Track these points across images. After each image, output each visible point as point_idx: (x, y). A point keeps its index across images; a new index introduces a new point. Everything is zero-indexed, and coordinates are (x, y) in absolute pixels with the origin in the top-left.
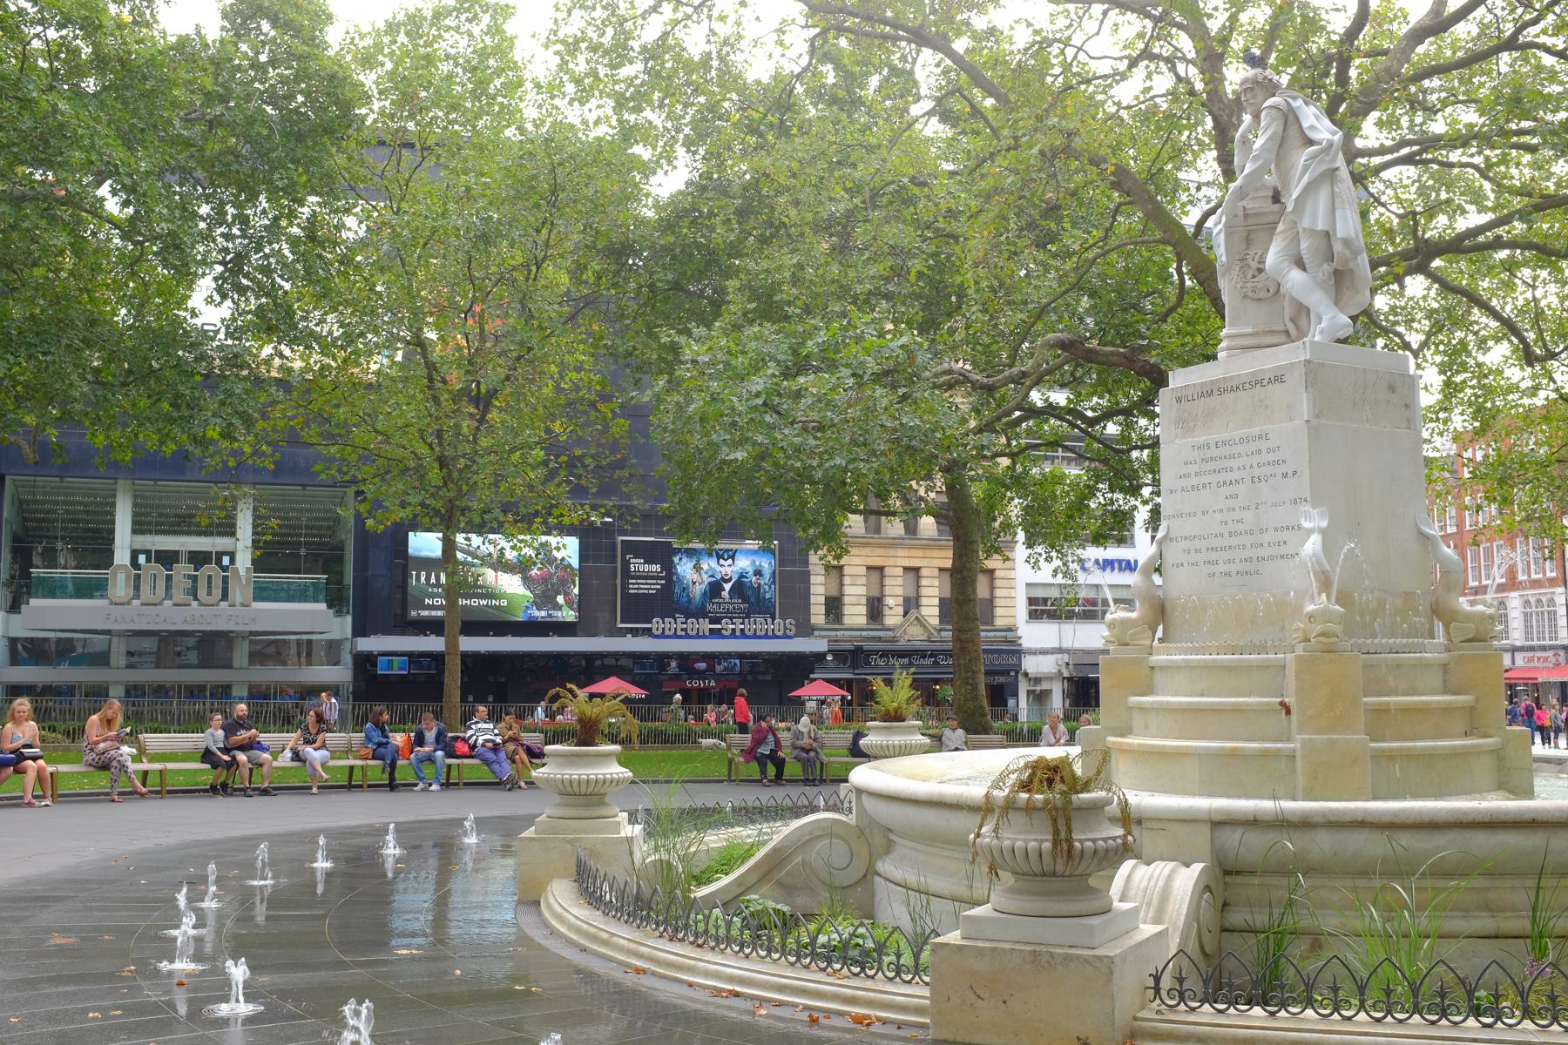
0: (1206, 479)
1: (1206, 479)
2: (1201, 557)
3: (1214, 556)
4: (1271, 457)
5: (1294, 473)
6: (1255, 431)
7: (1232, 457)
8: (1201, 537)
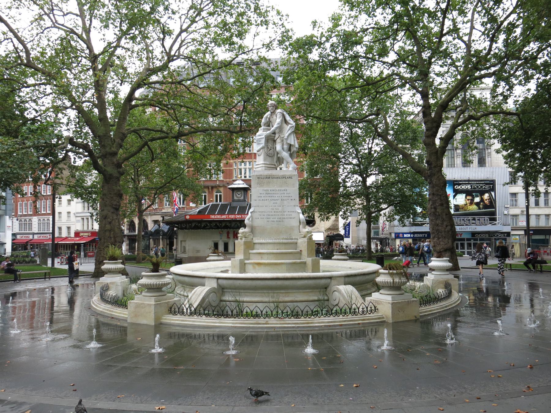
0: (266, 198)
3: (269, 217)
4: (288, 195)
6: (283, 188)
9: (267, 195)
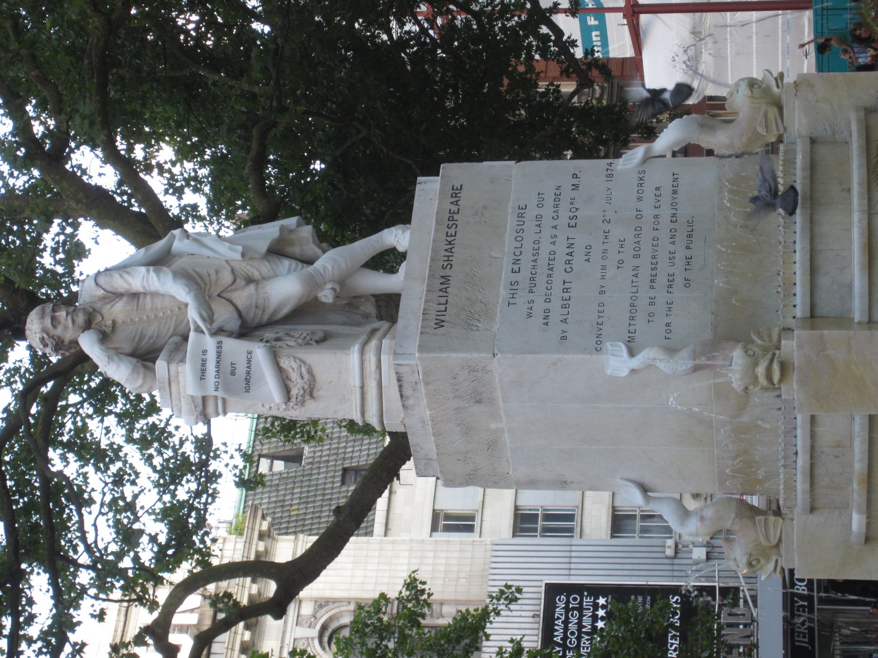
0: (558, 286)
1: (558, 286)
2: (662, 296)
3: (662, 280)
4: (549, 202)
5: (575, 176)
6: (511, 221)
7: (536, 252)
8: (634, 298)
9: (541, 288)
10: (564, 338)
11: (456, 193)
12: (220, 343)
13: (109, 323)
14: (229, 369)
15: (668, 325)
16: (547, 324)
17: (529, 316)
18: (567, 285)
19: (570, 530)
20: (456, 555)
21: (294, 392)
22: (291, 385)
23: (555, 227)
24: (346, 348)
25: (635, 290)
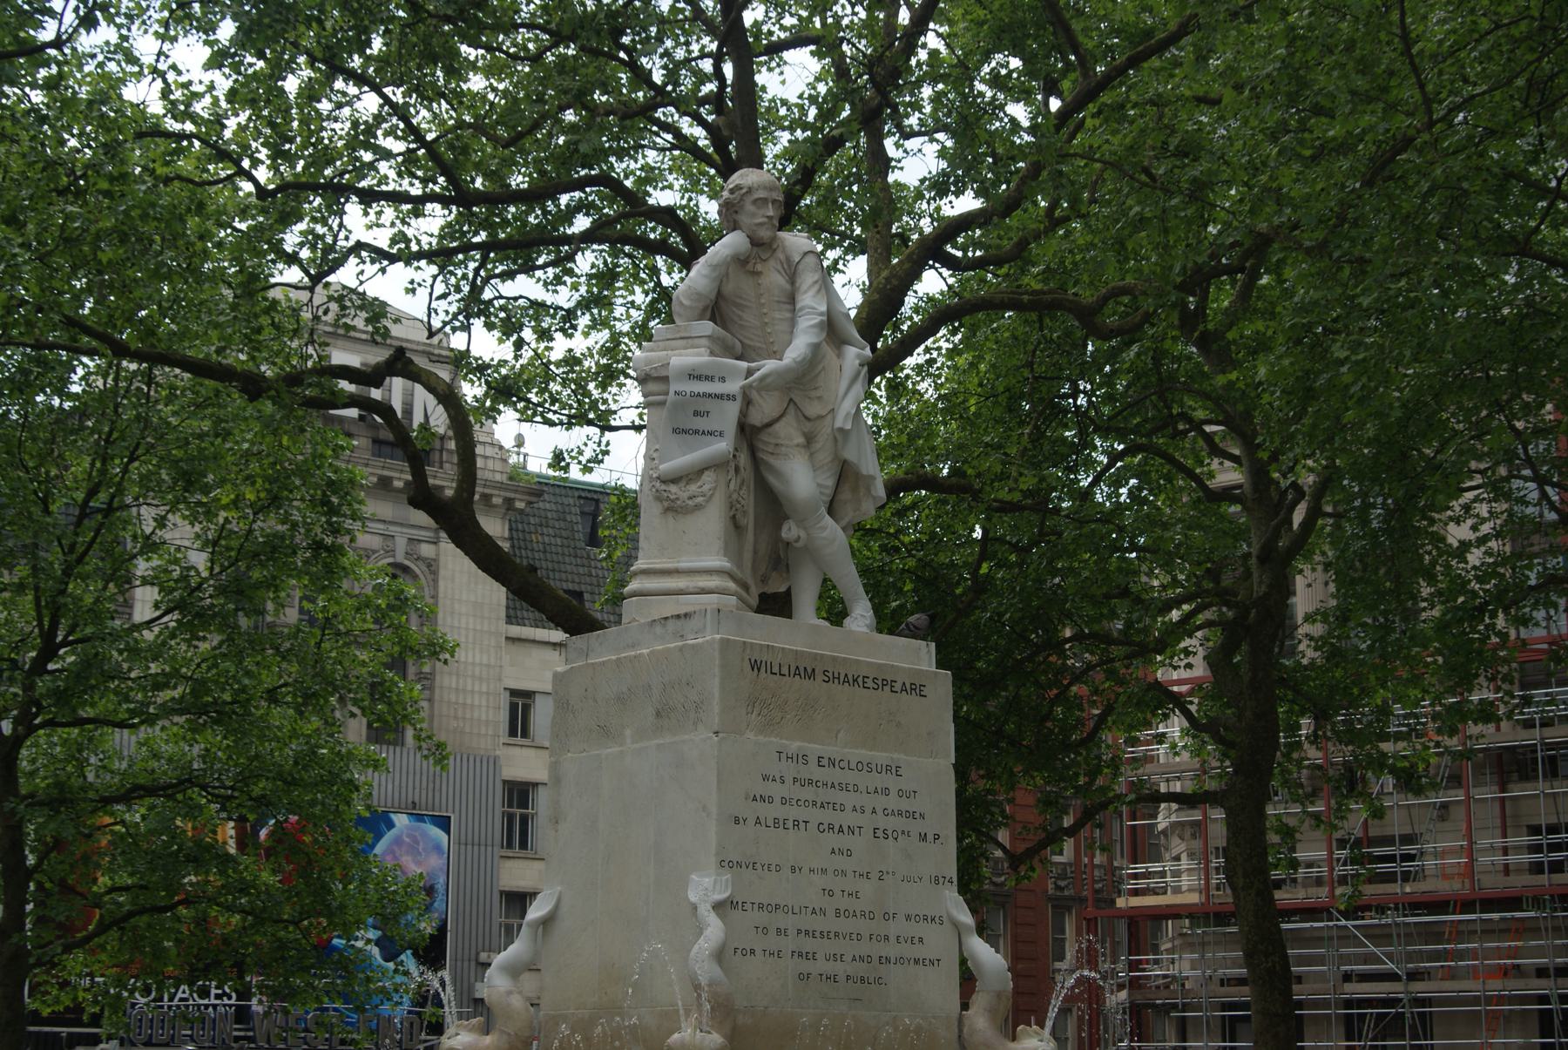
2: (789, 944)
3: (808, 945)
4: (905, 805)
5: (937, 837)
6: (881, 757)
7: (843, 787)
10: (737, 821)
11: (916, 689)
12: (734, 398)
13: (759, 267)
14: (702, 409)
15: (753, 952)
16: (755, 799)
17: (765, 778)
18: (802, 825)
19: (510, 845)
20: (484, 717)
21: (673, 488)
22: (682, 484)
23: (874, 811)
24: (726, 553)
25: (796, 910)
